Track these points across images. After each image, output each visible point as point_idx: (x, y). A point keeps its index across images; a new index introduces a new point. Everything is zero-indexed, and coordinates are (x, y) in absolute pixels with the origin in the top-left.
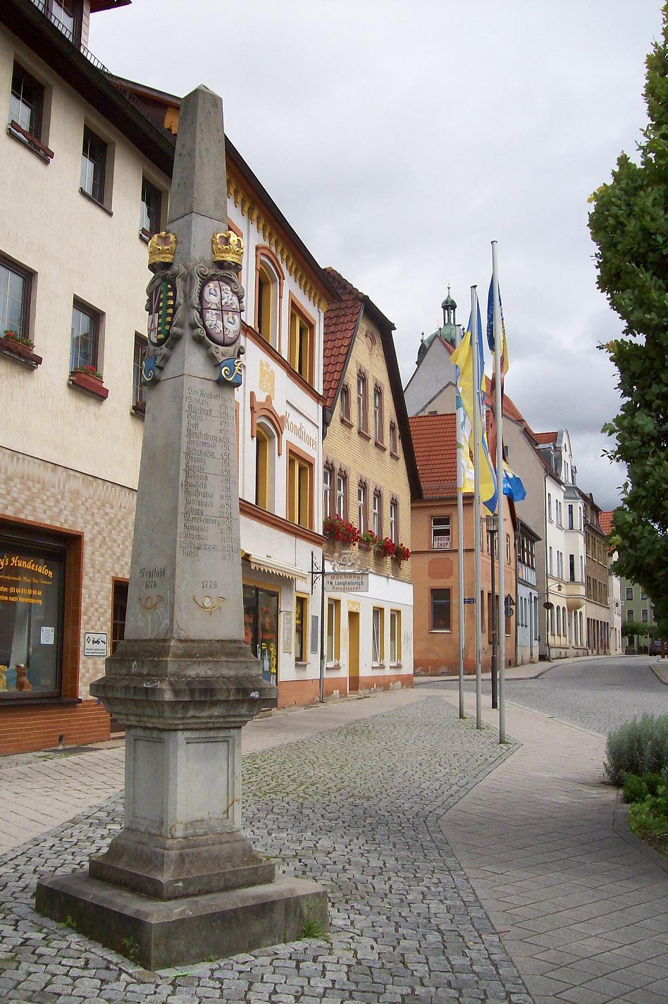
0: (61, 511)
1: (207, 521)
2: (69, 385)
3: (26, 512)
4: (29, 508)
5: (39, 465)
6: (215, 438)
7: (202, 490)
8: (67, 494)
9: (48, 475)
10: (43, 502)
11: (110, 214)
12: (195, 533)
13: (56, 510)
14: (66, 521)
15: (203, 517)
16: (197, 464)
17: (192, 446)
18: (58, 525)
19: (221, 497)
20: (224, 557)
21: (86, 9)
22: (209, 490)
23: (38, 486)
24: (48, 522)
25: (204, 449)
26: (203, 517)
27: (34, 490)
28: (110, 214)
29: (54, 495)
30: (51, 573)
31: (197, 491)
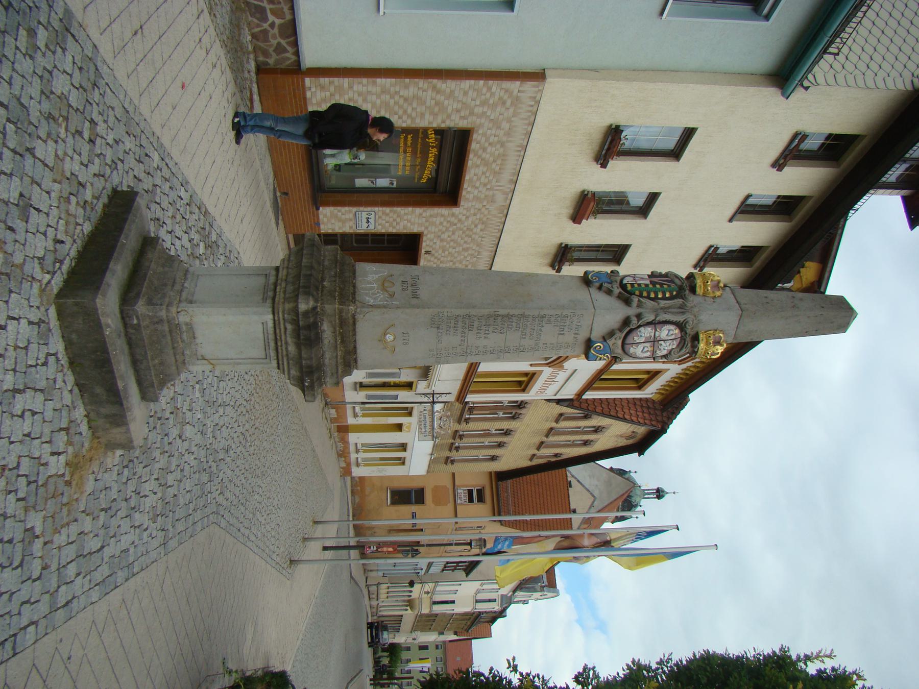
0: (477, 188)
1: (463, 335)
2: (584, 191)
3: (475, 159)
4: (479, 162)
5: (515, 169)
6: (538, 339)
7: (491, 329)
8: (491, 193)
9: (507, 176)
10: (483, 173)
11: (730, 220)
12: (452, 325)
13: (478, 184)
14: (468, 193)
15: (466, 331)
16: (514, 324)
17: (530, 319)
18: (465, 186)
19: (485, 347)
20: (430, 350)
21: (905, 192)
22: (491, 336)
23: (497, 169)
24: (467, 178)
25: (528, 330)
26: (466, 331)
27: (494, 165)
28: (730, 220)
29: (490, 182)
30: (425, 181)
31: (490, 325)
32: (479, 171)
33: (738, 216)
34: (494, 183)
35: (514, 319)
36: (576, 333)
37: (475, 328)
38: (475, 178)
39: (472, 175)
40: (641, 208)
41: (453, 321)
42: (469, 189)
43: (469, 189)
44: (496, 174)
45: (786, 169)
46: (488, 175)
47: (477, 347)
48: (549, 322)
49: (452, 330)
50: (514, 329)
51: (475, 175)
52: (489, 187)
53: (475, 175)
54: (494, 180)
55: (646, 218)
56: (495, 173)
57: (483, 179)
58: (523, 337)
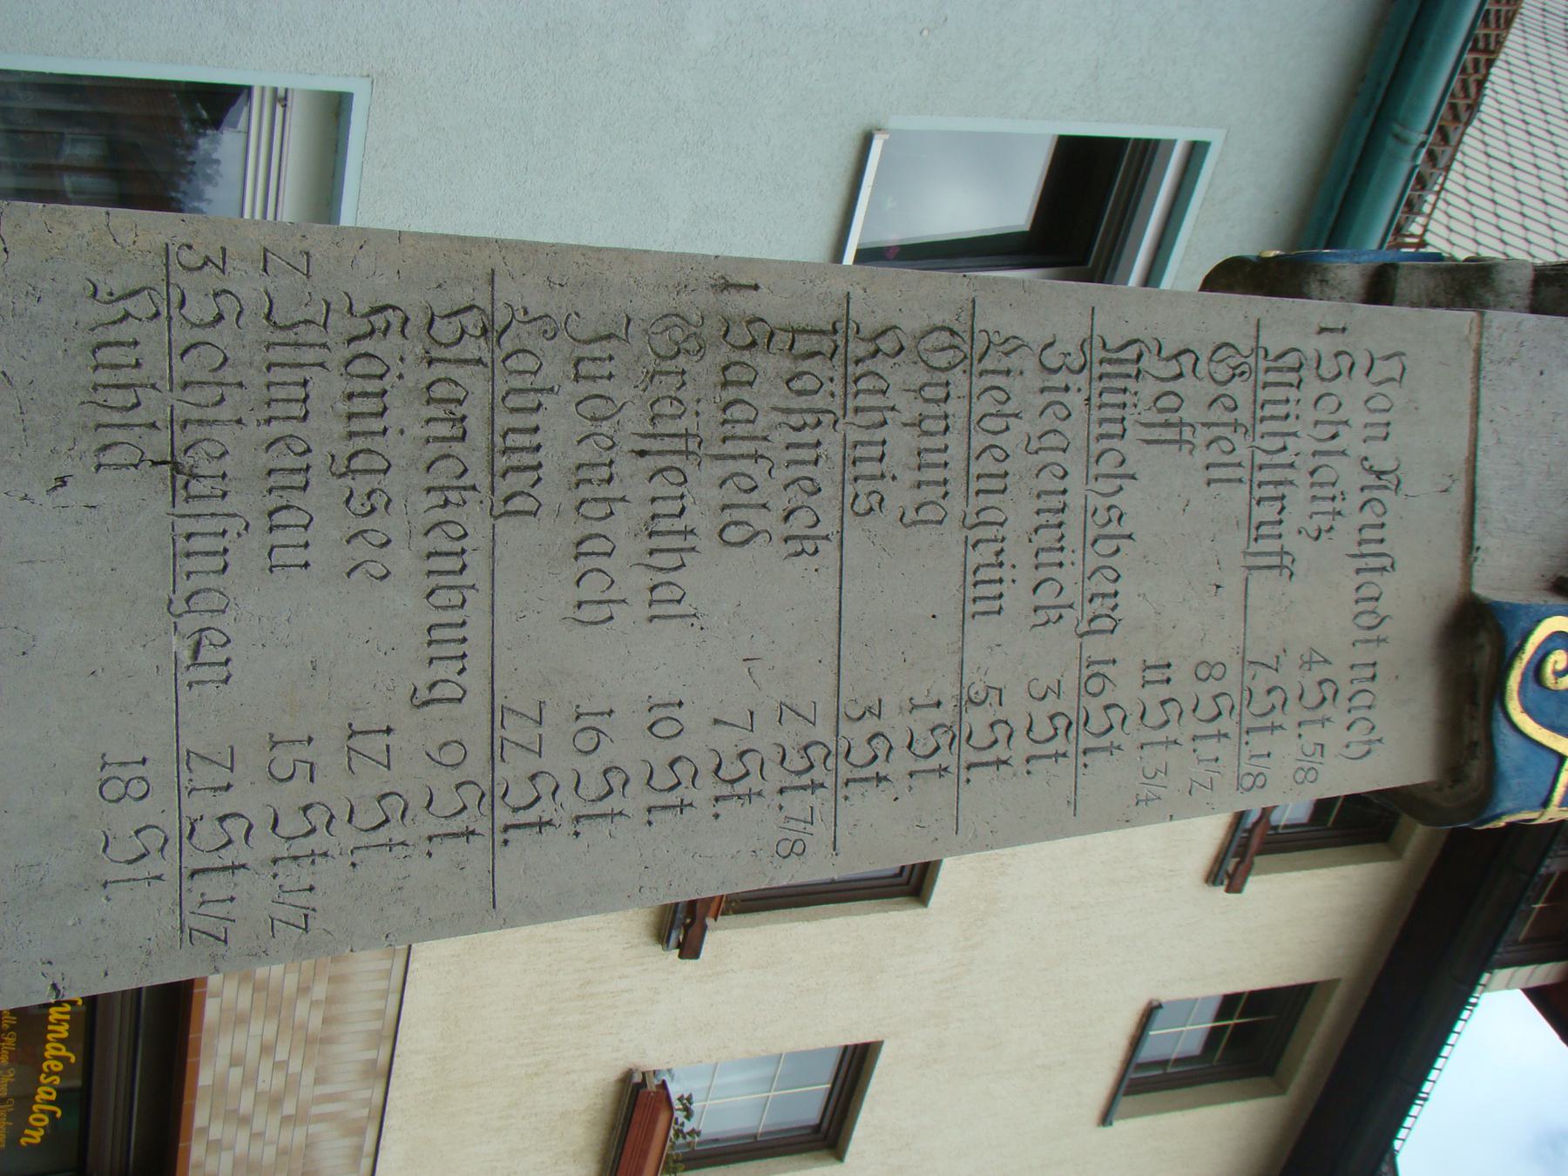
0: (245, 1121)
1: (446, 567)
2: (629, 1074)
3: (230, 989)
4: (244, 1001)
5: (381, 1014)
6: (1102, 618)
7: (705, 489)
8: (299, 1135)
9: (352, 1051)
10: (267, 1049)
11: (1106, 1119)
12: (326, 433)
13: (246, 1103)
14: (215, 1146)
15: (474, 517)
16: (901, 442)
17: (1024, 389)
18: (201, 1117)
19: (662, 715)
20: (114, 779)
21: (1543, 974)
22: (712, 577)
23: (315, 1022)
24: (205, 1078)
25: (1019, 512)
26: (474, 517)
27: (302, 1008)
28: (1106, 1119)
29: (292, 1084)
30: (37, 1136)
31: (690, 446)
32: (247, 1040)
33: (1125, 1102)
34: (307, 1089)
35: (901, 374)
36: (1373, 559)
37: (554, 491)
38: (236, 1074)
39: (222, 1063)
40: (817, 1128)
41: (328, 387)
42: (215, 1132)
43: (215, 1132)
44: (316, 1043)
45: (1254, 884)
46: (281, 1055)
47: (591, 726)
48: (1171, 430)
49: (324, 494)
50: (899, 497)
51: (236, 1061)
52: (289, 1108)
53: (236, 1061)
54: (308, 1077)
55: (840, 1157)
56: (309, 1041)
57: (269, 1080)
58: (980, 595)
